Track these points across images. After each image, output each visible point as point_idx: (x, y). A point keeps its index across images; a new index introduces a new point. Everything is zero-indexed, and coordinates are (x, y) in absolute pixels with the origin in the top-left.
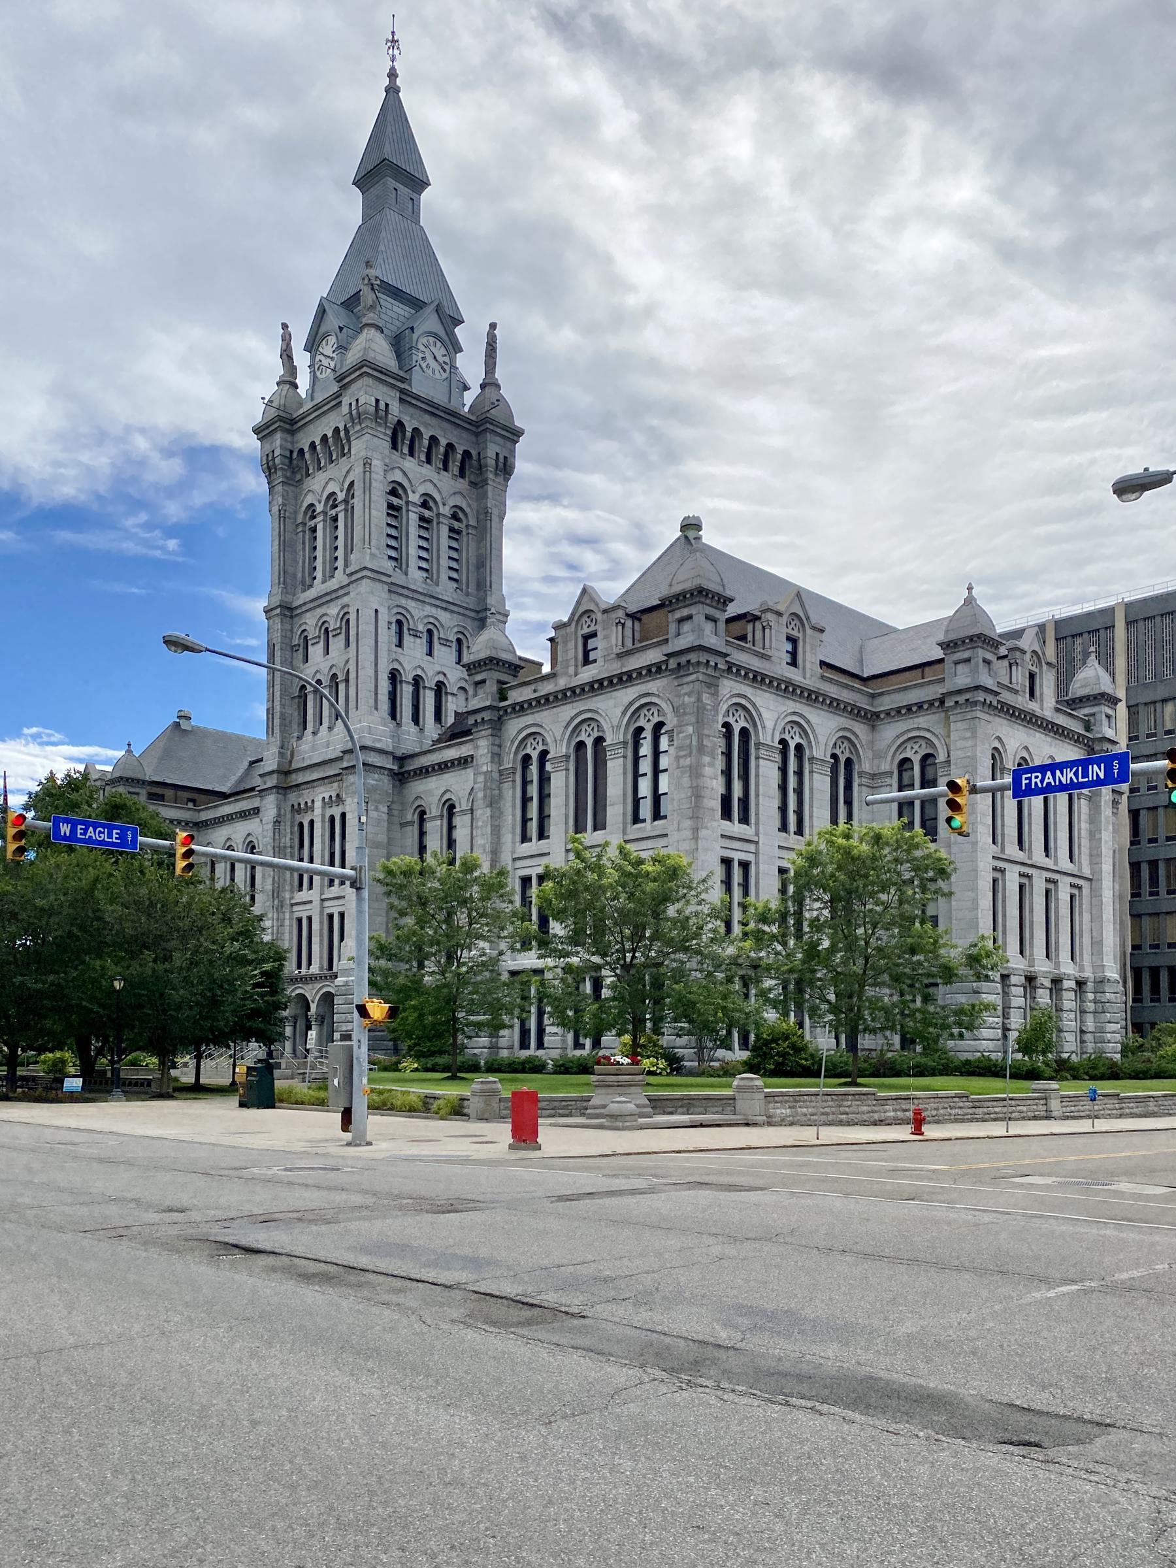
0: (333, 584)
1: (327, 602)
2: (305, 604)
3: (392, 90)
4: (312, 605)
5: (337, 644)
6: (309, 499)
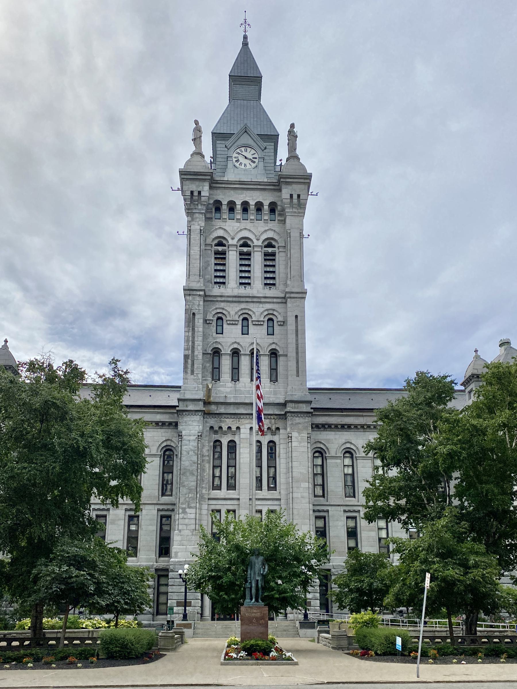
0: (243, 291)
1: (247, 302)
2: (221, 296)
3: (245, 44)
6: (220, 233)
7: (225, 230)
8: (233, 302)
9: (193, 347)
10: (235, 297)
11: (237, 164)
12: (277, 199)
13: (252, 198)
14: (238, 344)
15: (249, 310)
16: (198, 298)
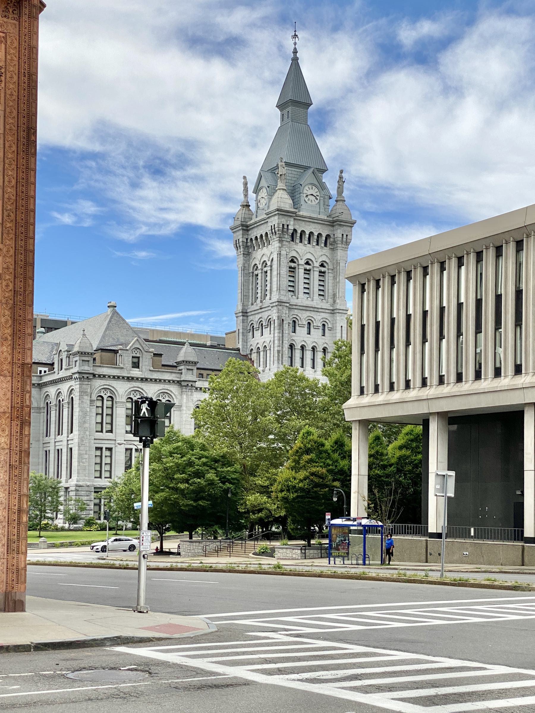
1: (310, 311)
2: (296, 305)
4: (301, 308)
5: (316, 333)
6: (294, 254)
7: (297, 252)
8: (302, 310)
9: (282, 344)
10: (304, 306)
11: (306, 200)
12: (330, 232)
13: (316, 229)
14: (305, 342)
15: (312, 317)
16: (285, 308)
